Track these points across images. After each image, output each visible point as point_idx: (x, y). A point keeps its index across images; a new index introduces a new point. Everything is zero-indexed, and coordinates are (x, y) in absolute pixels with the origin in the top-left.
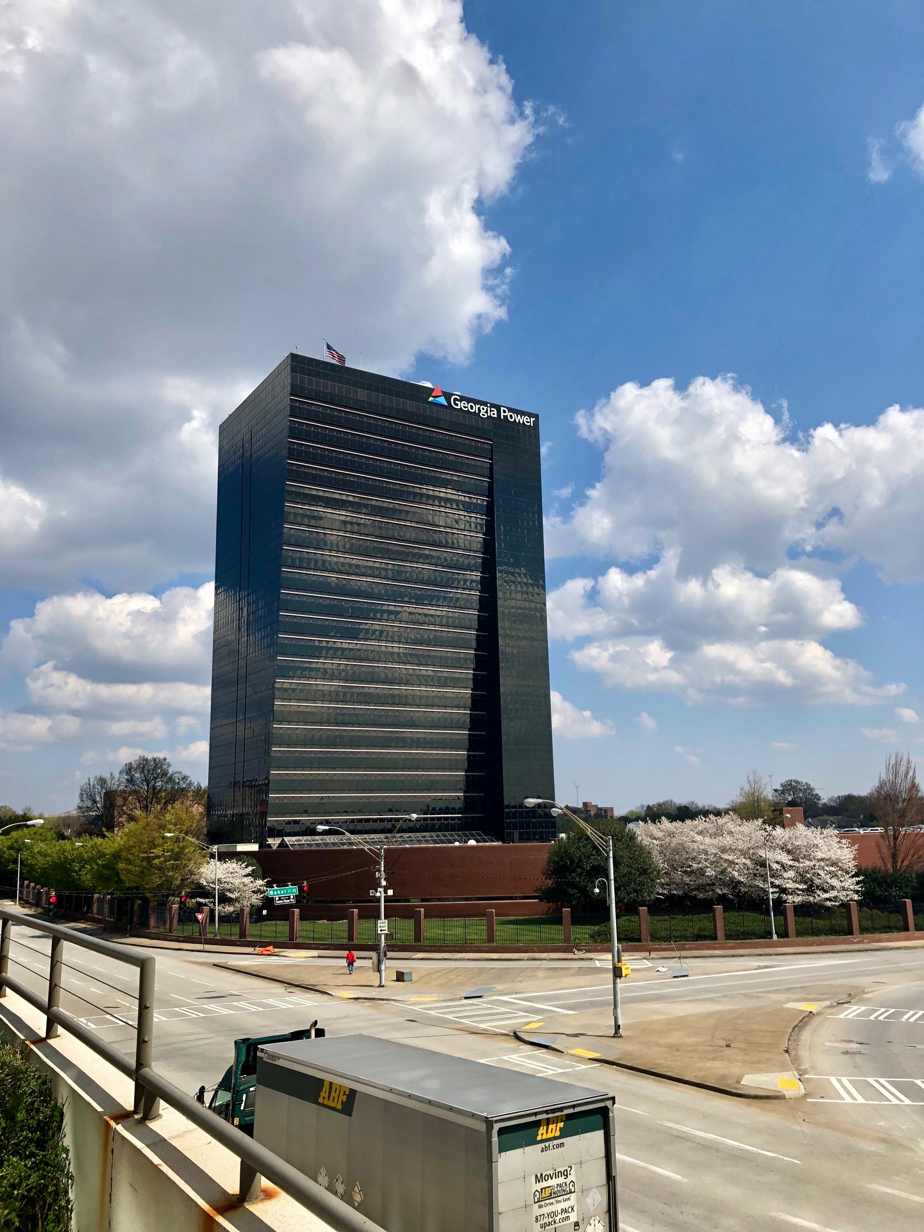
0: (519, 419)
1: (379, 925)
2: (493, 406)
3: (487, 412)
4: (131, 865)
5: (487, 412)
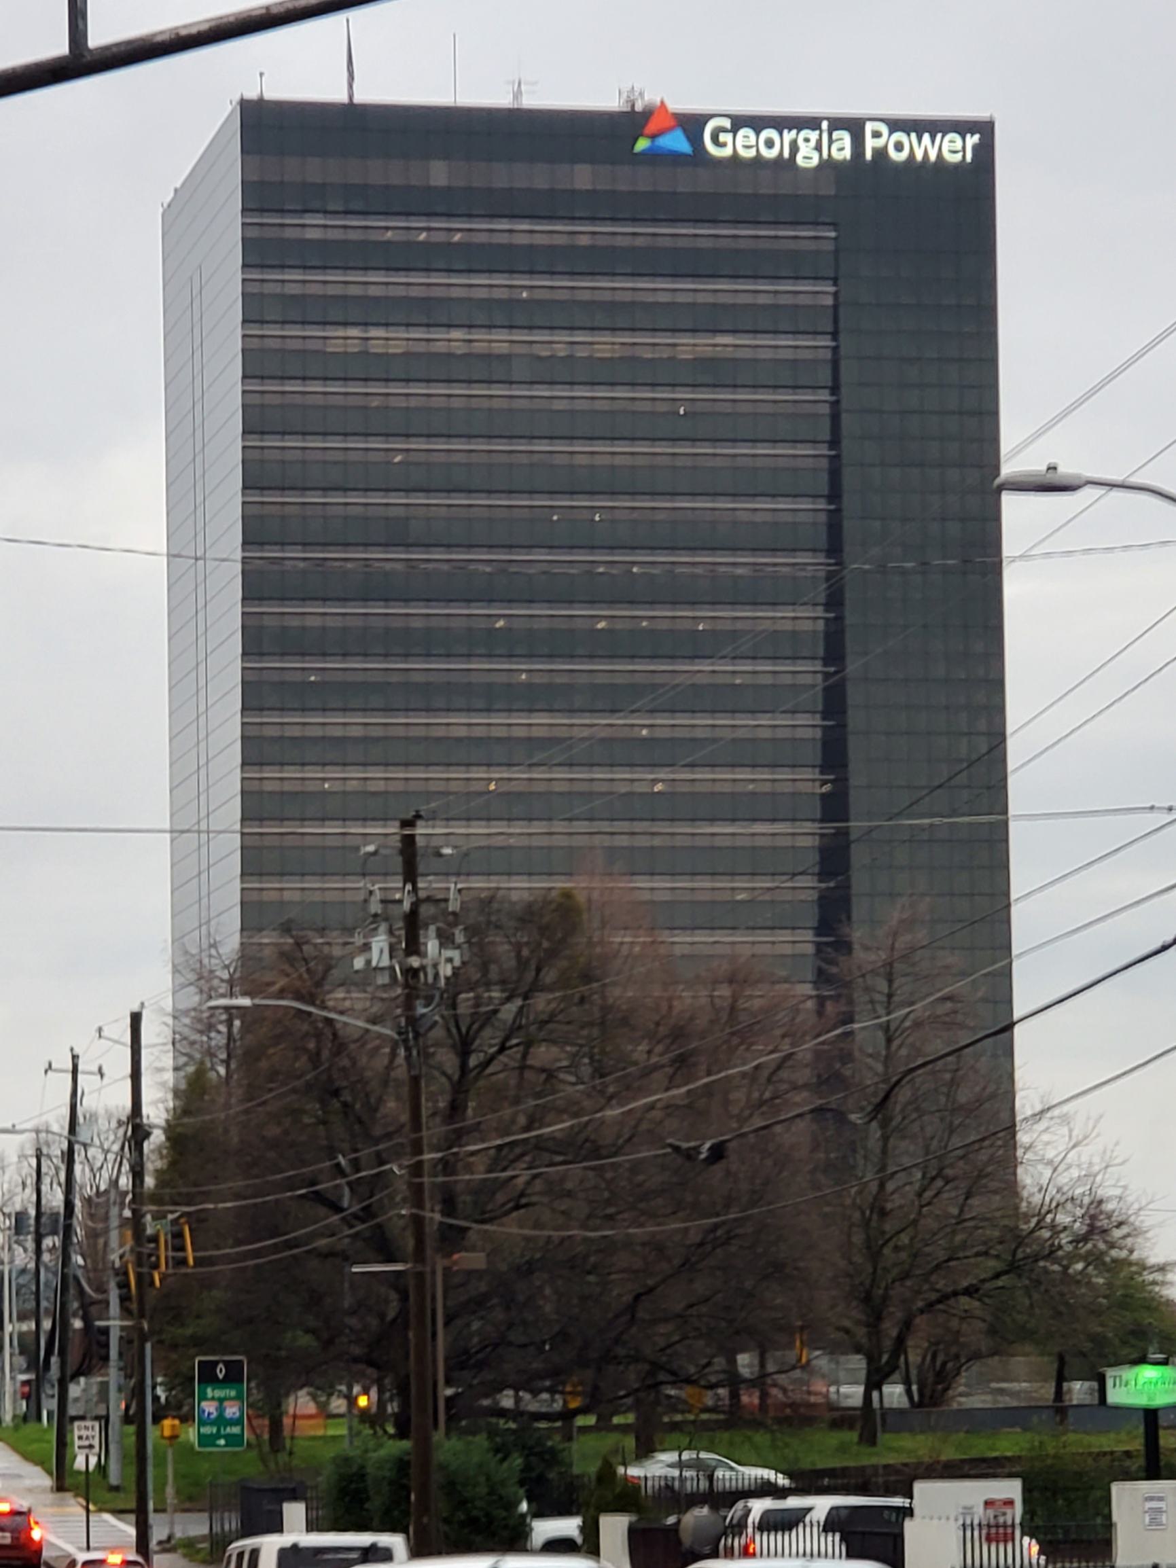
0: (925, 148)
1: (76, 1433)
2: (837, 124)
3: (818, 148)
4: (494, 1193)
5: (818, 148)
